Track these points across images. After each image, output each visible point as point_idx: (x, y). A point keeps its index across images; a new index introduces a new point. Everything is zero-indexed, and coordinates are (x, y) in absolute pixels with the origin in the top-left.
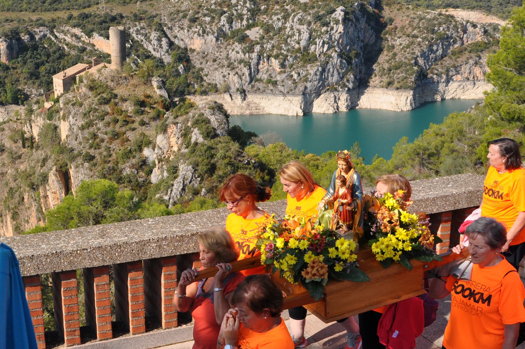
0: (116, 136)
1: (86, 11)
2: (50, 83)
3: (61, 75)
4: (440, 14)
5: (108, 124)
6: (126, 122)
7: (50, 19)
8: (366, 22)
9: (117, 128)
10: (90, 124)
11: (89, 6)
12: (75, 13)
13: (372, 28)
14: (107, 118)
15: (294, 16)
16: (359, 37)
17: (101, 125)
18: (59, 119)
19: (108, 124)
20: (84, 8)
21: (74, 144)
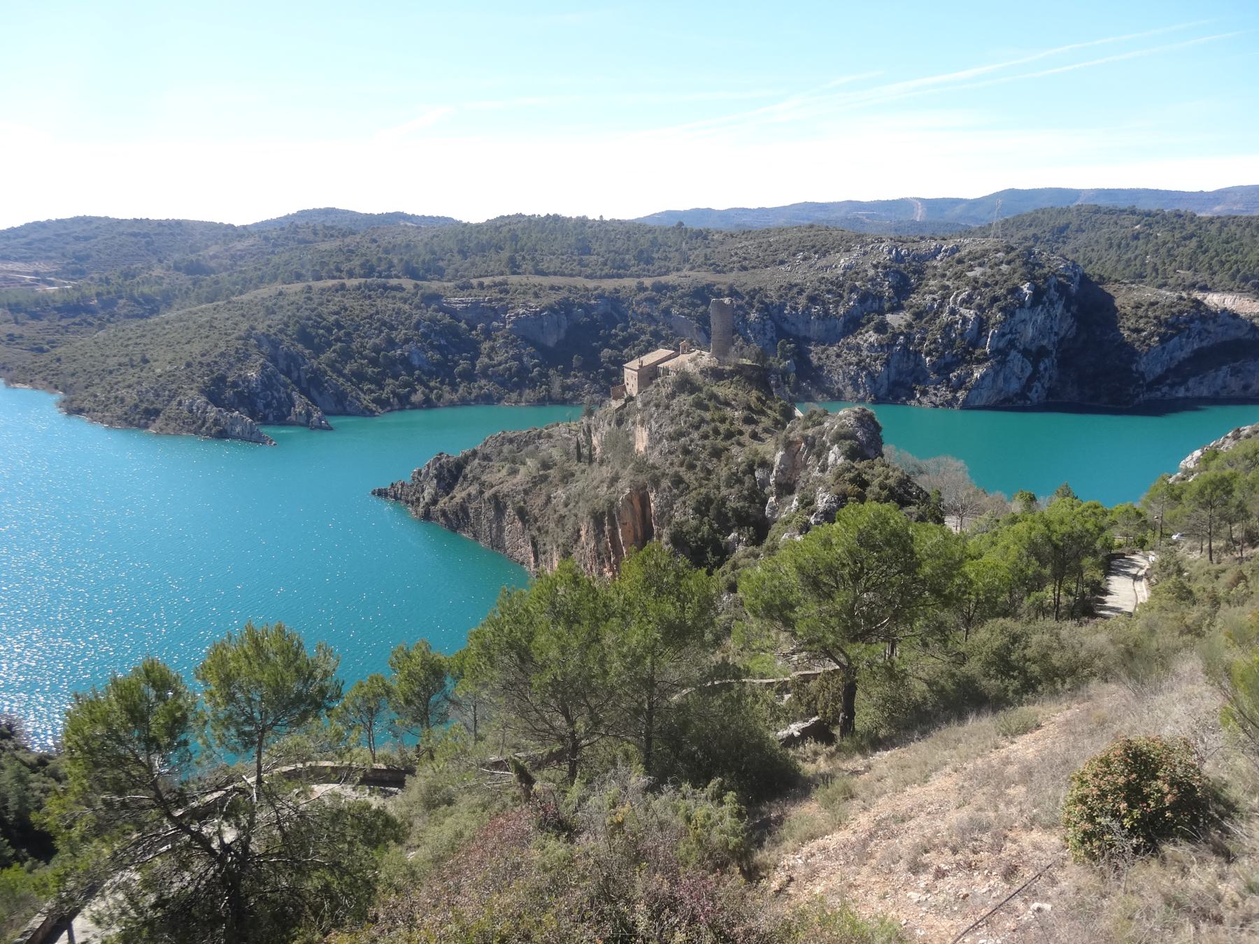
0: (717, 453)
1: (663, 279)
2: (619, 374)
3: (635, 364)
4: (1181, 298)
5: (705, 437)
6: (729, 435)
7: (612, 288)
8: (1064, 306)
9: (720, 443)
10: (680, 434)
11: (666, 274)
12: (648, 282)
13: (1073, 315)
14: (704, 428)
15: (957, 296)
16: (1052, 328)
17: (695, 435)
18: (634, 423)
19: (705, 437)
20: (659, 275)
21: (654, 458)
